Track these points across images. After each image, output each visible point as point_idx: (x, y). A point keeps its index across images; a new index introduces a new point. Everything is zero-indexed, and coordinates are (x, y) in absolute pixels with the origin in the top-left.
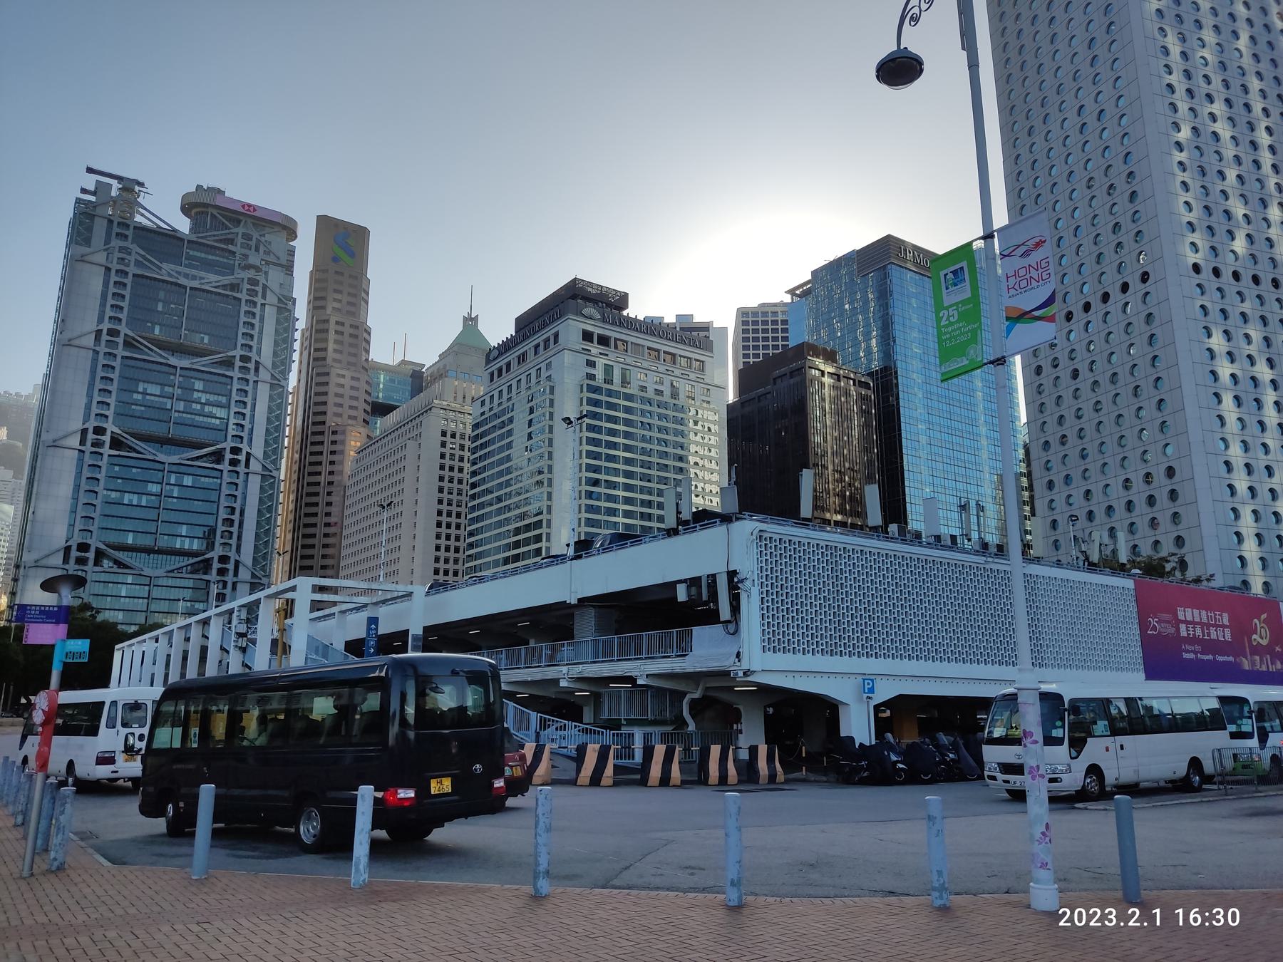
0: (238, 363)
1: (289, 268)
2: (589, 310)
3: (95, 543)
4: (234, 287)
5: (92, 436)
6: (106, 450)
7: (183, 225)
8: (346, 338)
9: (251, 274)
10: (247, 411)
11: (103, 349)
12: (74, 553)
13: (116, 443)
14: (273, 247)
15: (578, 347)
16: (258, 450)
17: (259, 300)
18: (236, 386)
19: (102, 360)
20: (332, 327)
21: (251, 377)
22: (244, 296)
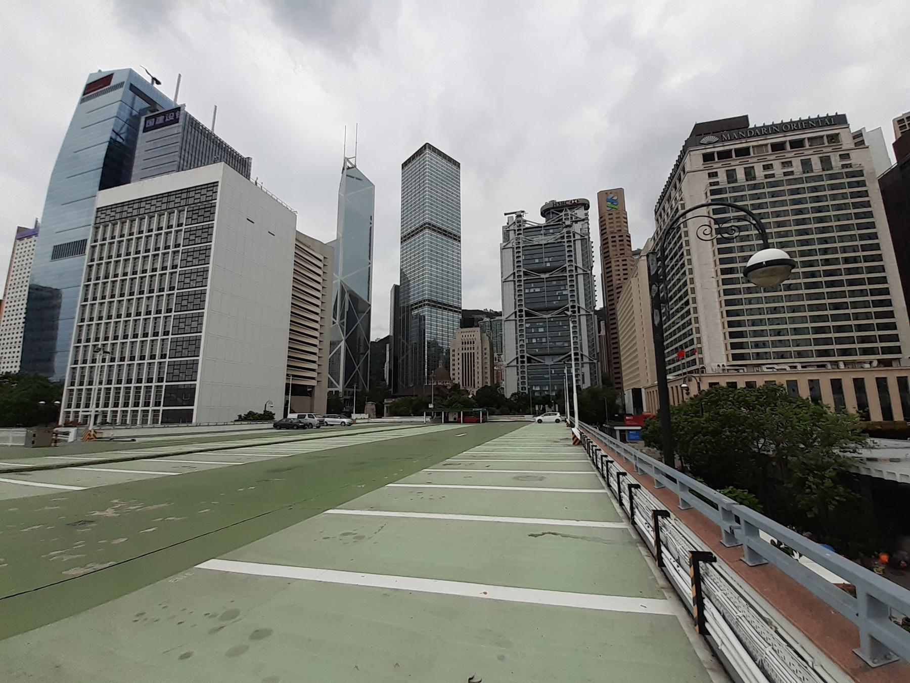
0: (568, 269)
1: (586, 220)
2: (705, 140)
3: (526, 355)
4: (563, 237)
5: (518, 313)
6: (524, 318)
7: (542, 221)
8: (618, 243)
9: (565, 230)
10: (575, 289)
11: (516, 279)
12: (520, 360)
13: (528, 314)
14: (578, 215)
15: (702, 168)
16: (583, 305)
17: (572, 239)
18: (569, 279)
19: (517, 284)
20: (610, 240)
21: (574, 273)
22: (566, 240)
